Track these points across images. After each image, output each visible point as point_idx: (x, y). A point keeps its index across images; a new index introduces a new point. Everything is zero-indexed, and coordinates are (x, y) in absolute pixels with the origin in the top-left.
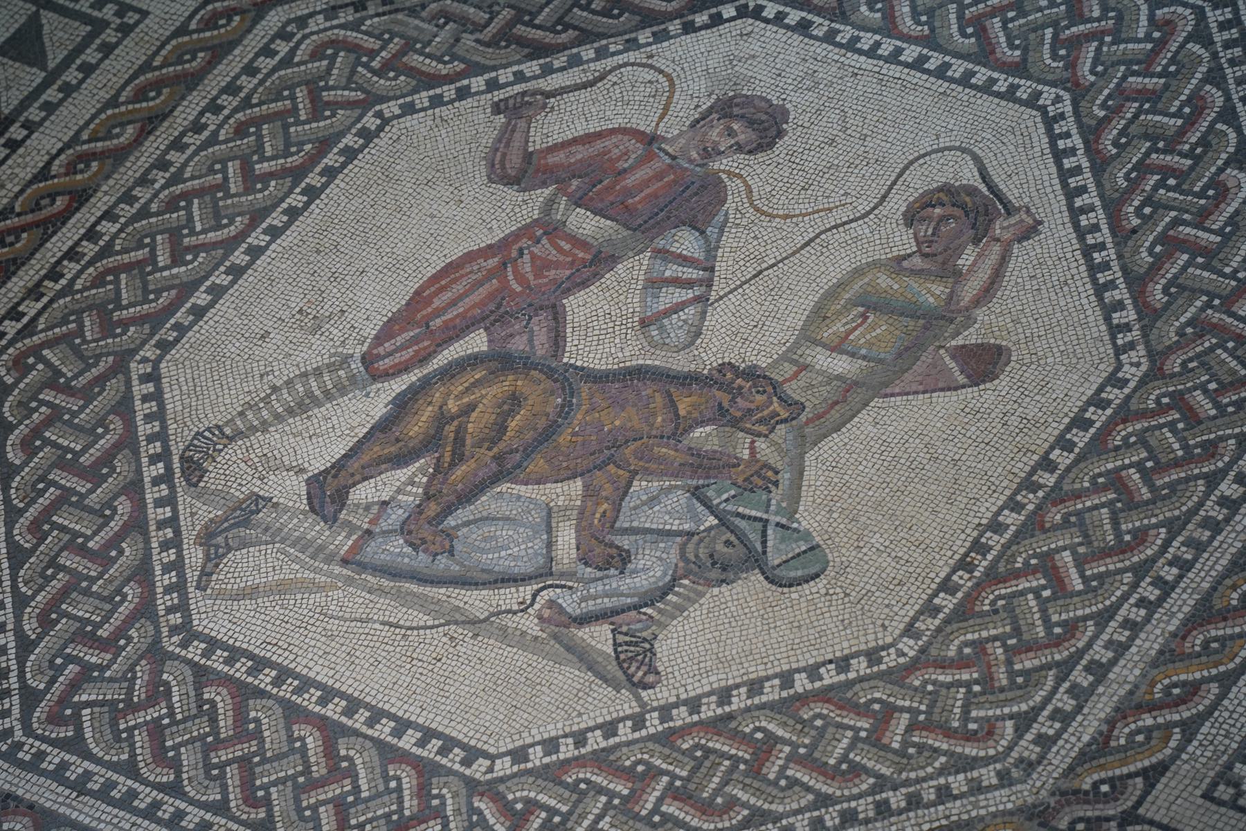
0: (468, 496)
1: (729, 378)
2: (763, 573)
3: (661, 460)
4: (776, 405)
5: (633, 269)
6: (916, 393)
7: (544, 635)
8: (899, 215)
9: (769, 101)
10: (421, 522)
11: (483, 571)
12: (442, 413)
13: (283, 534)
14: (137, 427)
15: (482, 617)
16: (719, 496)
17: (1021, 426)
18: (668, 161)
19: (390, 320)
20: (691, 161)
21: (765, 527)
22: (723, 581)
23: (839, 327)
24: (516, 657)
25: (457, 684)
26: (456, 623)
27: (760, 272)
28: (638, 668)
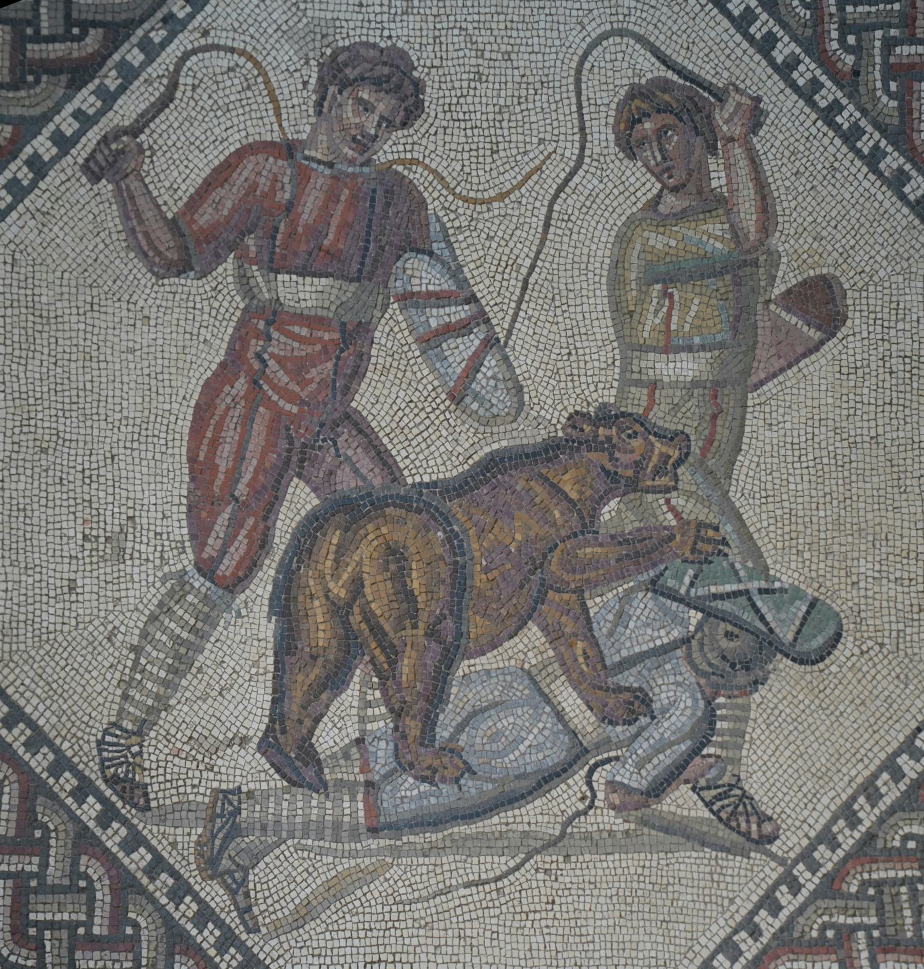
0: (436, 696)
1: (593, 430)
2: (787, 656)
3: (593, 563)
4: (658, 445)
5: (392, 332)
6: (782, 370)
7: (633, 826)
8: (613, 149)
9: (375, 46)
10: (413, 747)
11: (518, 777)
12: (333, 603)
13: (285, 827)
14: (27, 764)
15: (557, 833)
16: (681, 582)
17: (908, 368)
18: (328, 172)
19: (190, 508)
20: (352, 162)
21: (750, 599)
22: (756, 682)
23: (651, 321)
24: (624, 864)
25: (591, 922)
26: (538, 851)
27: (526, 282)
28: (748, 821)
